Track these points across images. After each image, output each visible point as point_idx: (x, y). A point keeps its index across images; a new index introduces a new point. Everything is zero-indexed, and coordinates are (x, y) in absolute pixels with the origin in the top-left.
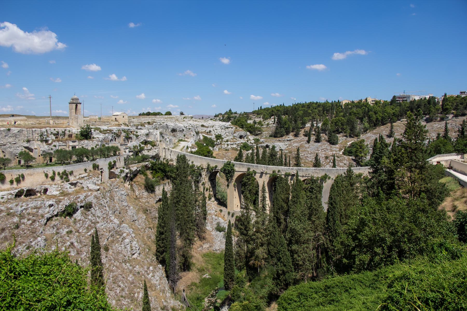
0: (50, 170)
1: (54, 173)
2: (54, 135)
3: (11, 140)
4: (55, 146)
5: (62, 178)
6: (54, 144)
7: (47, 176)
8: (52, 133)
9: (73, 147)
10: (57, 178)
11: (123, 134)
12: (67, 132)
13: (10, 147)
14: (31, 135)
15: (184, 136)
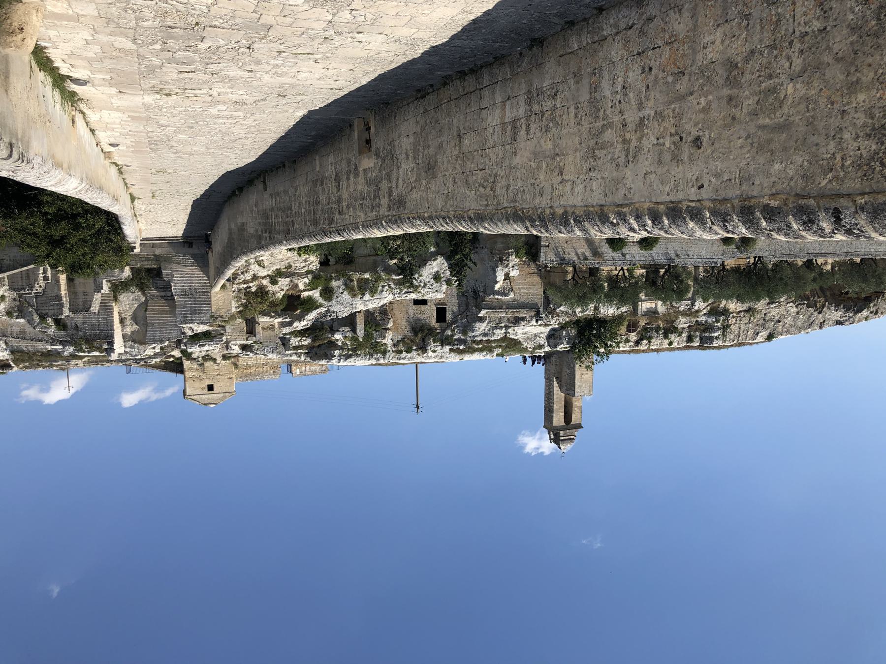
8: (680, 335)
12: (633, 337)
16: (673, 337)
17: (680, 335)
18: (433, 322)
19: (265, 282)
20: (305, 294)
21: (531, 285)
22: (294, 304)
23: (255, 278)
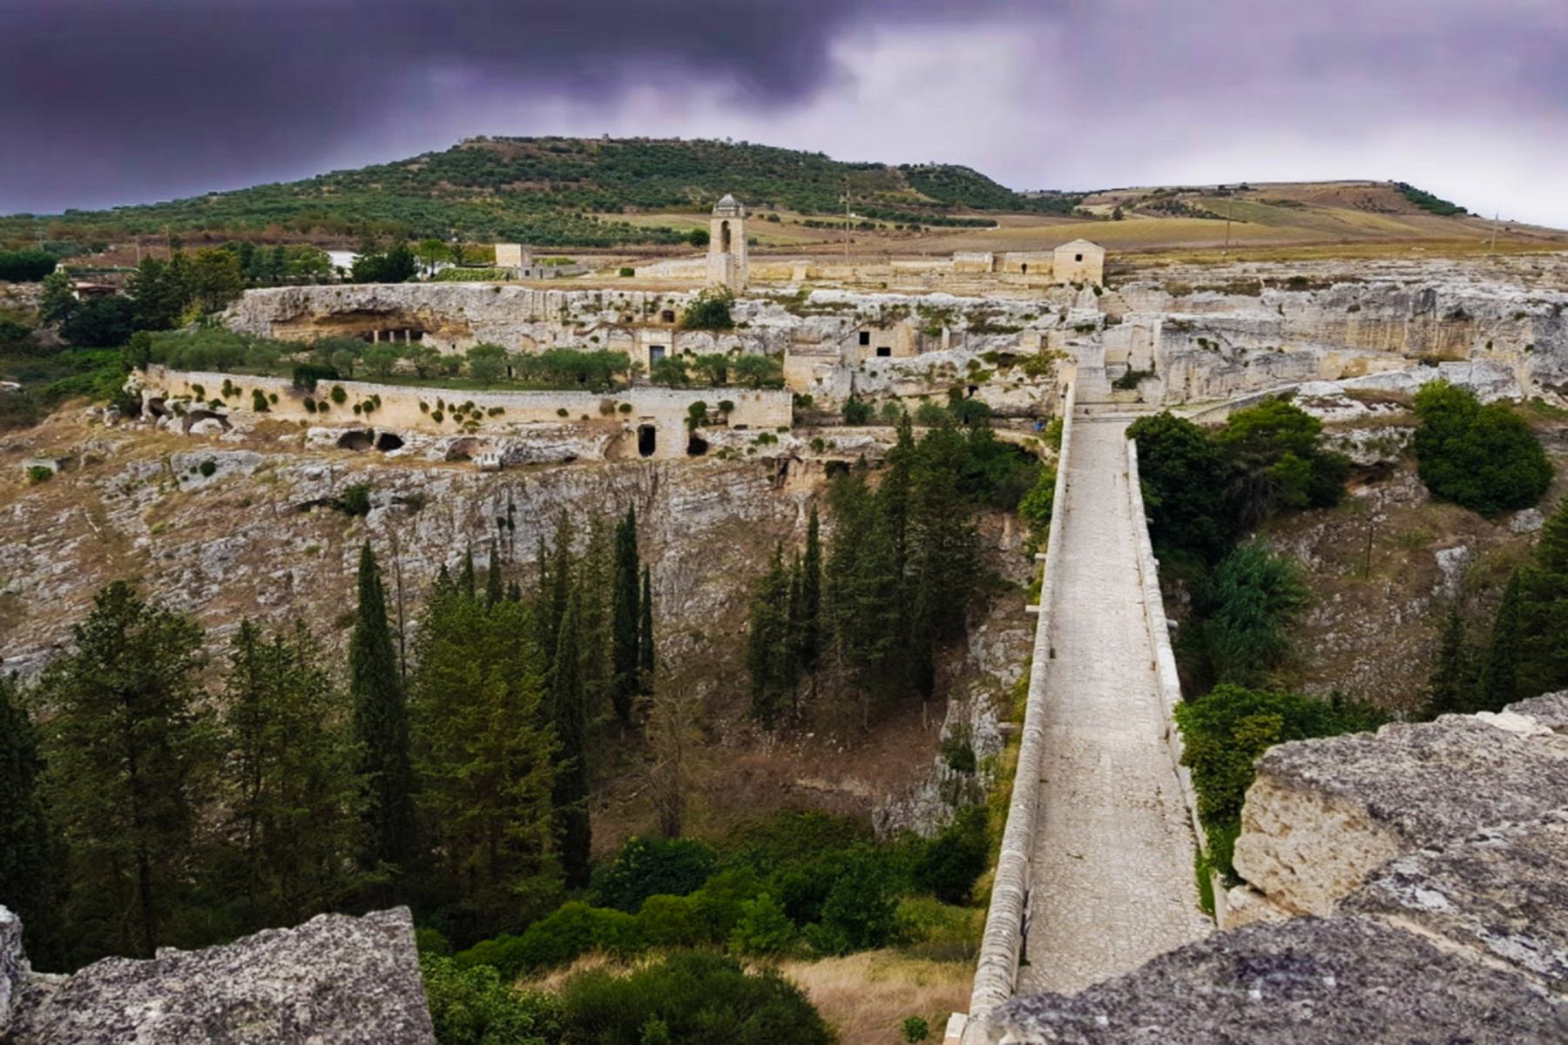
0: (431, 395)
1: (441, 404)
2: (618, 309)
3: (499, 314)
4: (596, 339)
5: (458, 419)
6: (596, 333)
7: (424, 407)
8: (611, 303)
9: (652, 348)
10: (448, 417)
11: (914, 319)
12: (664, 306)
13: (492, 333)
14: (541, 306)
15: (1489, 346)
16: (620, 302)
17: (611, 303)
18: (874, 332)
19: (1028, 381)
20: (995, 366)
21: (797, 374)
22: (1005, 360)
23: (1038, 385)
